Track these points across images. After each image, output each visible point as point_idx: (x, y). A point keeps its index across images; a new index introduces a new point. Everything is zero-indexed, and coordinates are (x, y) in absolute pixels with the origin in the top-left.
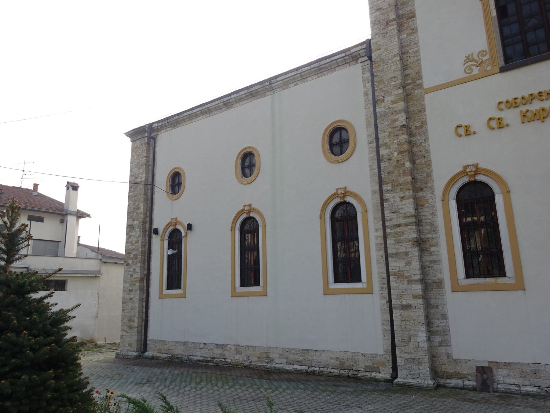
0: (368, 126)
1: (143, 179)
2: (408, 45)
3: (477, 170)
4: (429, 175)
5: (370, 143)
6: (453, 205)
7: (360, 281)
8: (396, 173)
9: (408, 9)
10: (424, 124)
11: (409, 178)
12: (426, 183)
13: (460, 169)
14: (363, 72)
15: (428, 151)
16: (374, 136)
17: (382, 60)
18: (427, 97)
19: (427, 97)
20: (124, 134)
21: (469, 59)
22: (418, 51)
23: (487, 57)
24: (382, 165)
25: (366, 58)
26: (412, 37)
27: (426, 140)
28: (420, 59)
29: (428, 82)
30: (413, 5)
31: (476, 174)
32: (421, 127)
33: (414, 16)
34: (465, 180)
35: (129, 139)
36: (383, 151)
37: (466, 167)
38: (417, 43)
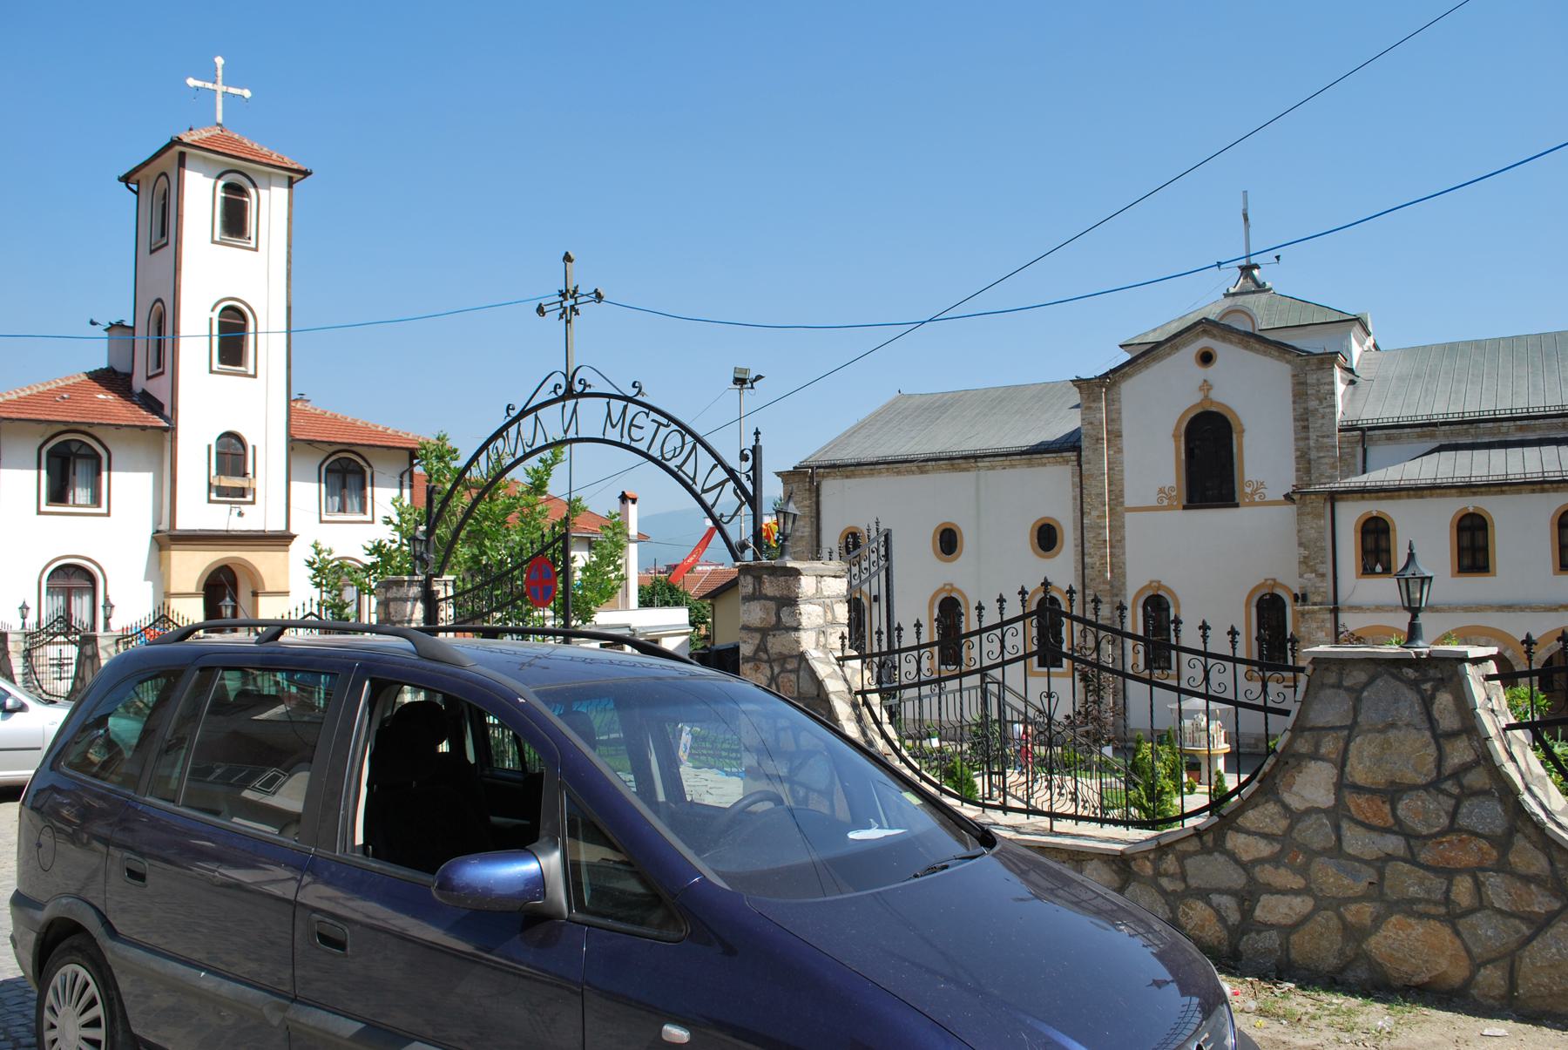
0: (1075, 529)
1: (806, 534)
2: (1115, 463)
3: (1160, 586)
4: (1124, 584)
5: (1076, 546)
6: (1140, 611)
7: (1061, 666)
8: (1098, 581)
9: (1116, 427)
10: (1123, 538)
11: (1108, 587)
12: (1121, 590)
13: (1146, 583)
14: (1073, 477)
15: (1124, 564)
16: (1080, 541)
17: (1091, 476)
18: (1128, 516)
19: (1128, 516)
20: (779, 474)
21: (1161, 491)
22: (1122, 471)
23: (1174, 493)
24: (1086, 571)
25: (1076, 463)
26: (1118, 456)
27: (1124, 554)
28: (1122, 479)
29: (1130, 500)
30: (1121, 425)
31: (1158, 589)
32: (1120, 541)
33: (1121, 436)
34: (1150, 593)
35: (780, 479)
36: (1087, 560)
37: (1151, 582)
38: (1122, 463)
